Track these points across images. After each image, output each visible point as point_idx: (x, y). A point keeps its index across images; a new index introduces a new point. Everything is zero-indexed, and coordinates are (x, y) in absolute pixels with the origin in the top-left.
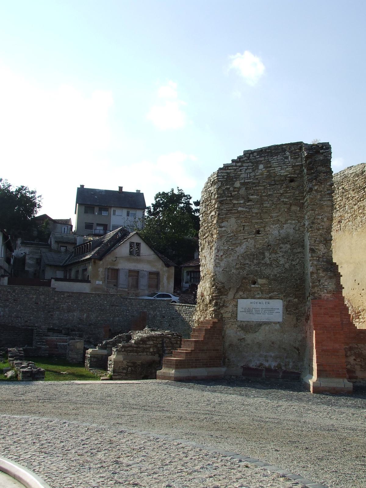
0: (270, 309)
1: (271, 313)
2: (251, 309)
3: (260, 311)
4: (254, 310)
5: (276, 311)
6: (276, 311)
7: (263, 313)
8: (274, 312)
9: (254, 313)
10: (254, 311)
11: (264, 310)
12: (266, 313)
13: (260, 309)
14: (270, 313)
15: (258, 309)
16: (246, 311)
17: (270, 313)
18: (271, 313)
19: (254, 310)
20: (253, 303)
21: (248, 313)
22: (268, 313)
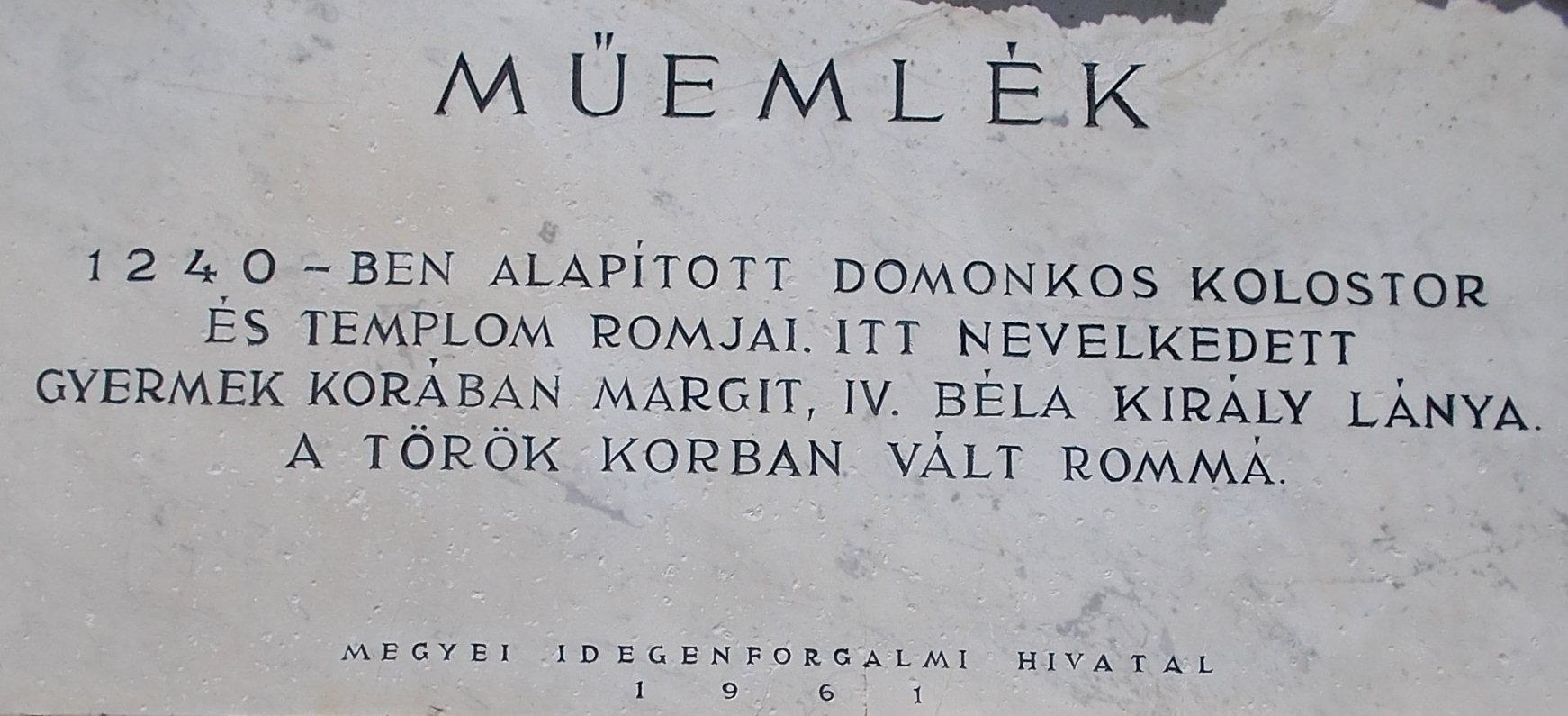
0: (1176, 309)
1: (1234, 441)
2: (470, 290)
3: (822, 375)
4: (568, 312)
5: (1395, 351)
6: (1395, 351)
7: (913, 419)
8: (1328, 385)
9: (580, 428)
10: (573, 359)
11: (941, 314)
12: (1042, 443)
13: (811, 299)
14: (1183, 440)
15: (715, 307)
16: (290, 359)
17: (1183, 440)
18: (1234, 441)
19: (568, 312)
20: (543, 82)
21: (344, 430)
22: (1094, 426)
